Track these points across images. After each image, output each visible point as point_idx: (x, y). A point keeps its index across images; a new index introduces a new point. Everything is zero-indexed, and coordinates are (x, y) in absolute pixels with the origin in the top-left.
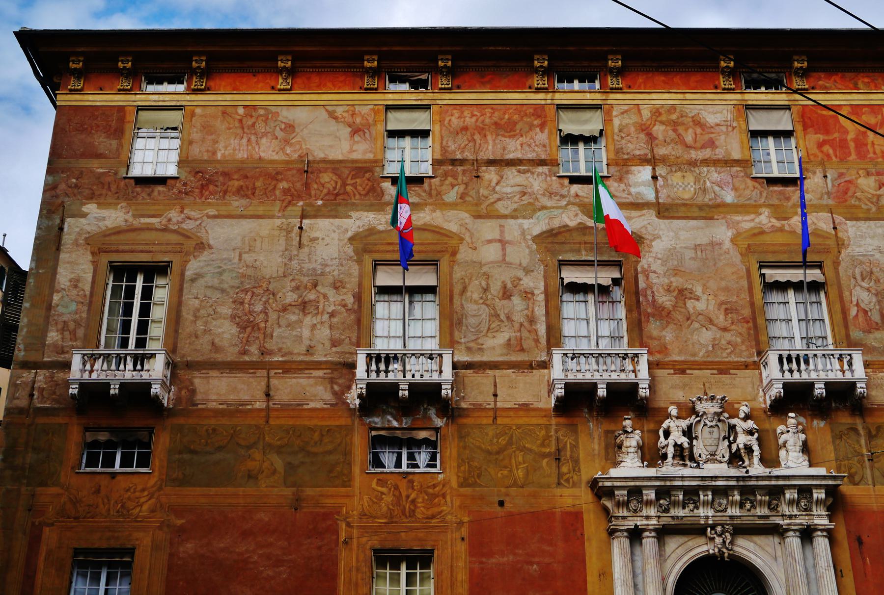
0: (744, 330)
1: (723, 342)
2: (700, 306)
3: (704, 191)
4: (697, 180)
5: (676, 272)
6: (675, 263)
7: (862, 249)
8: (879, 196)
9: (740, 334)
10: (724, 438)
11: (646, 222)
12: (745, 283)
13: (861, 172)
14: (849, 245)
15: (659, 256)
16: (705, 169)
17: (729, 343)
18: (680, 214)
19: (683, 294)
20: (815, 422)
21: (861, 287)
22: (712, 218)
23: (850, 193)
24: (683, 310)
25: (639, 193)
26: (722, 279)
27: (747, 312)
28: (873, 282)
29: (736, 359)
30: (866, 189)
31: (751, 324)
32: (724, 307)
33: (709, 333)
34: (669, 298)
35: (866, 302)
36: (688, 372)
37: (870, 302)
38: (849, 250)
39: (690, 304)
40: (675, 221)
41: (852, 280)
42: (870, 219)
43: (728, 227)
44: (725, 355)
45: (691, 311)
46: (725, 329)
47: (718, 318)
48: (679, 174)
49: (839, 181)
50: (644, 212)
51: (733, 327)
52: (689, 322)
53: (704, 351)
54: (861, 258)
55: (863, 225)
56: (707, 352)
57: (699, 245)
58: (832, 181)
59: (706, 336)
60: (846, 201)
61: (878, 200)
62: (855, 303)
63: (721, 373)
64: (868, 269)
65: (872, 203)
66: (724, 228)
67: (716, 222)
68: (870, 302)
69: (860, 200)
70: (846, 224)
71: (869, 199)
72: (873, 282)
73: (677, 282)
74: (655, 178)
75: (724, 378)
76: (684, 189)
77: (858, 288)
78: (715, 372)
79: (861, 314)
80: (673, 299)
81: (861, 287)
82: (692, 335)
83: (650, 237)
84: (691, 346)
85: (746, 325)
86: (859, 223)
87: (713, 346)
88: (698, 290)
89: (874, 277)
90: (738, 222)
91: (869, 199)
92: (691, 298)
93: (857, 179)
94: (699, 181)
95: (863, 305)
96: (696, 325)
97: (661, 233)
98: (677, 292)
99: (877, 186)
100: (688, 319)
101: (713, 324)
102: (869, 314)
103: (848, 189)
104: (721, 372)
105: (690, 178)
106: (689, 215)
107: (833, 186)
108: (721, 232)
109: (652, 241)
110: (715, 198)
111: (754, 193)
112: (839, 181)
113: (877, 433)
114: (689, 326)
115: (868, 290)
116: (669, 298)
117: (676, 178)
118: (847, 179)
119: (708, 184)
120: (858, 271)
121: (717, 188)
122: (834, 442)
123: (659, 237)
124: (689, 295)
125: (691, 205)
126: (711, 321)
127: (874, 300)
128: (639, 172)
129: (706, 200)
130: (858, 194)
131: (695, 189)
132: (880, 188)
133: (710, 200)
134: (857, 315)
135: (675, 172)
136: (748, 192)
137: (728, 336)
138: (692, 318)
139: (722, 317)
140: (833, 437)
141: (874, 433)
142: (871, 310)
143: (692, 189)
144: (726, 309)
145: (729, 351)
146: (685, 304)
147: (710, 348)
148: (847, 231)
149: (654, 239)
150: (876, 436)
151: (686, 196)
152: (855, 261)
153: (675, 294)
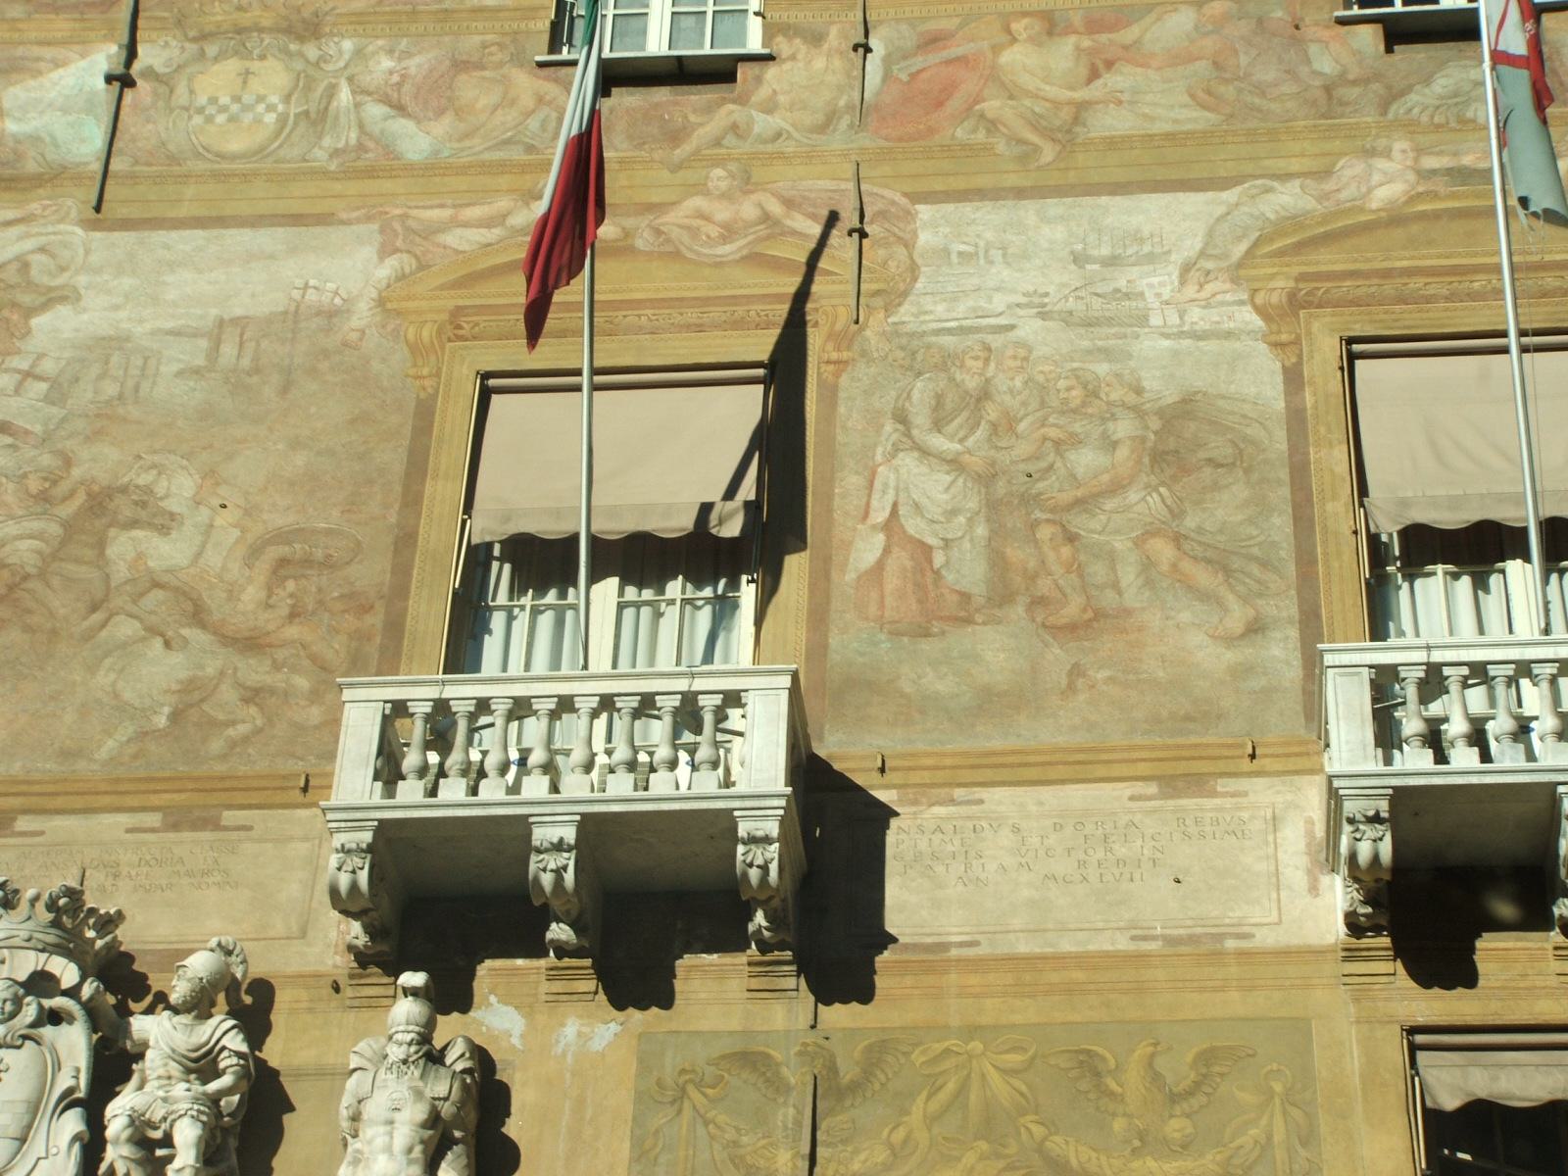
0: (339, 643)
1: (228, 694)
2: (168, 552)
3: (319, 119)
4: (303, 83)
5: (104, 421)
6: (110, 389)
7: (961, 309)
8: (1081, 108)
9: (314, 658)
10: (68, 1101)
11: (29, 244)
12: (393, 458)
13: (1017, 26)
14: (905, 294)
15: (48, 366)
16: (347, 45)
17: (253, 695)
18: (183, 211)
19: (103, 509)
20: (571, 1029)
21: (925, 452)
22: (324, 219)
23: (955, 104)
24: (83, 572)
25: (35, 139)
26: (295, 444)
27: (371, 573)
28: (981, 433)
29: (262, 766)
30: (1030, 82)
31: (376, 620)
32: (274, 552)
33: (176, 659)
34: (36, 525)
35: (935, 512)
36: (23, 823)
37: (953, 513)
38: (905, 313)
39: (122, 547)
40: (159, 236)
41: (889, 427)
42: (1020, 193)
43: (385, 251)
44: (216, 745)
45: (120, 572)
46: (251, 644)
47: (233, 594)
48: (233, 65)
49: (919, 62)
50: (34, 207)
51: (292, 632)
52: (97, 617)
53: (126, 730)
54: (947, 340)
55: (985, 220)
56: (142, 735)
57: (235, 321)
58: (888, 61)
59: (158, 672)
60: (931, 131)
61: (1076, 120)
62: (880, 516)
63: (175, 827)
64: (972, 383)
65: (1049, 134)
66: (368, 252)
67: (335, 234)
68: (953, 513)
69: (992, 125)
70: (909, 216)
71: (1035, 123)
72: (981, 433)
73: (99, 462)
74: (122, 81)
75: (191, 845)
76: (232, 119)
77: (908, 461)
78: (153, 819)
79: (901, 558)
80: (54, 529)
81: (925, 452)
82: (92, 669)
83: (26, 299)
84: (69, 717)
85: (350, 622)
86: (967, 209)
87: (175, 717)
88: (179, 488)
89: (992, 412)
90: (431, 231)
91: (1035, 123)
92: (134, 524)
93: (997, 49)
94: (308, 88)
95: (913, 526)
96: (125, 628)
97: (82, 280)
98: (80, 498)
99: (1083, 71)
100: (94, 608)
101: (203, 625)
102: (939, 559)
103: (949, 89)
104: (178, 820)
105: (272, 77)
106: (229, 210)
107: (887, 76)
108: (349, 269)
109: (30, 312)
110: (361, 147)
111: (533, 124)
112: (919, 62)
113: (868, 1074)
114: (88, 636)
115: (955, 464)
116: (36, 525)
117: (217, 80)
118: (958, 51)
119: (345, 95)
120: (921, 391)
121: (375, 111)
122: (638, 1120)
123: (66, 296)
124: (127, 512)
125: (246, 177)
126: (198, 615)
127: (972, 504)
128: (57, 64)
129: (320, 155)
130: (992, 106)
131: (282, 120)
132: (1094, 75)
133: (336, 153)
134: (880, 565)
135: (216, 59)
136: (510, 116)
137: (255, 671)
138: (117, 601)
139: (252, 594)
140: (640, 1097)
141: (848, 1072)
142: (947, 543)
143: (270, 118)
144: (283, 562)
145: (242, 729)
146: (101, 545)
147: (161, 721)
148: (909, 245)
149: (45, 307)
150: (855, 1087)
151: (235, 145)
152: (915, 355)
153: (67, 510)
